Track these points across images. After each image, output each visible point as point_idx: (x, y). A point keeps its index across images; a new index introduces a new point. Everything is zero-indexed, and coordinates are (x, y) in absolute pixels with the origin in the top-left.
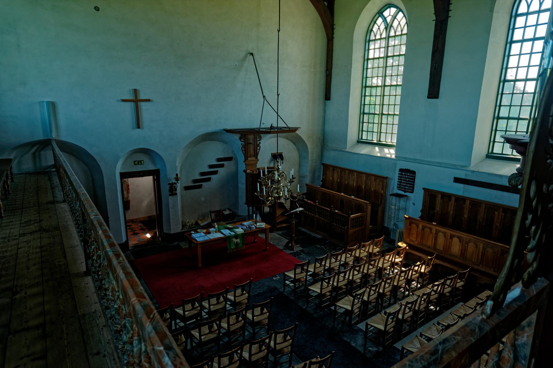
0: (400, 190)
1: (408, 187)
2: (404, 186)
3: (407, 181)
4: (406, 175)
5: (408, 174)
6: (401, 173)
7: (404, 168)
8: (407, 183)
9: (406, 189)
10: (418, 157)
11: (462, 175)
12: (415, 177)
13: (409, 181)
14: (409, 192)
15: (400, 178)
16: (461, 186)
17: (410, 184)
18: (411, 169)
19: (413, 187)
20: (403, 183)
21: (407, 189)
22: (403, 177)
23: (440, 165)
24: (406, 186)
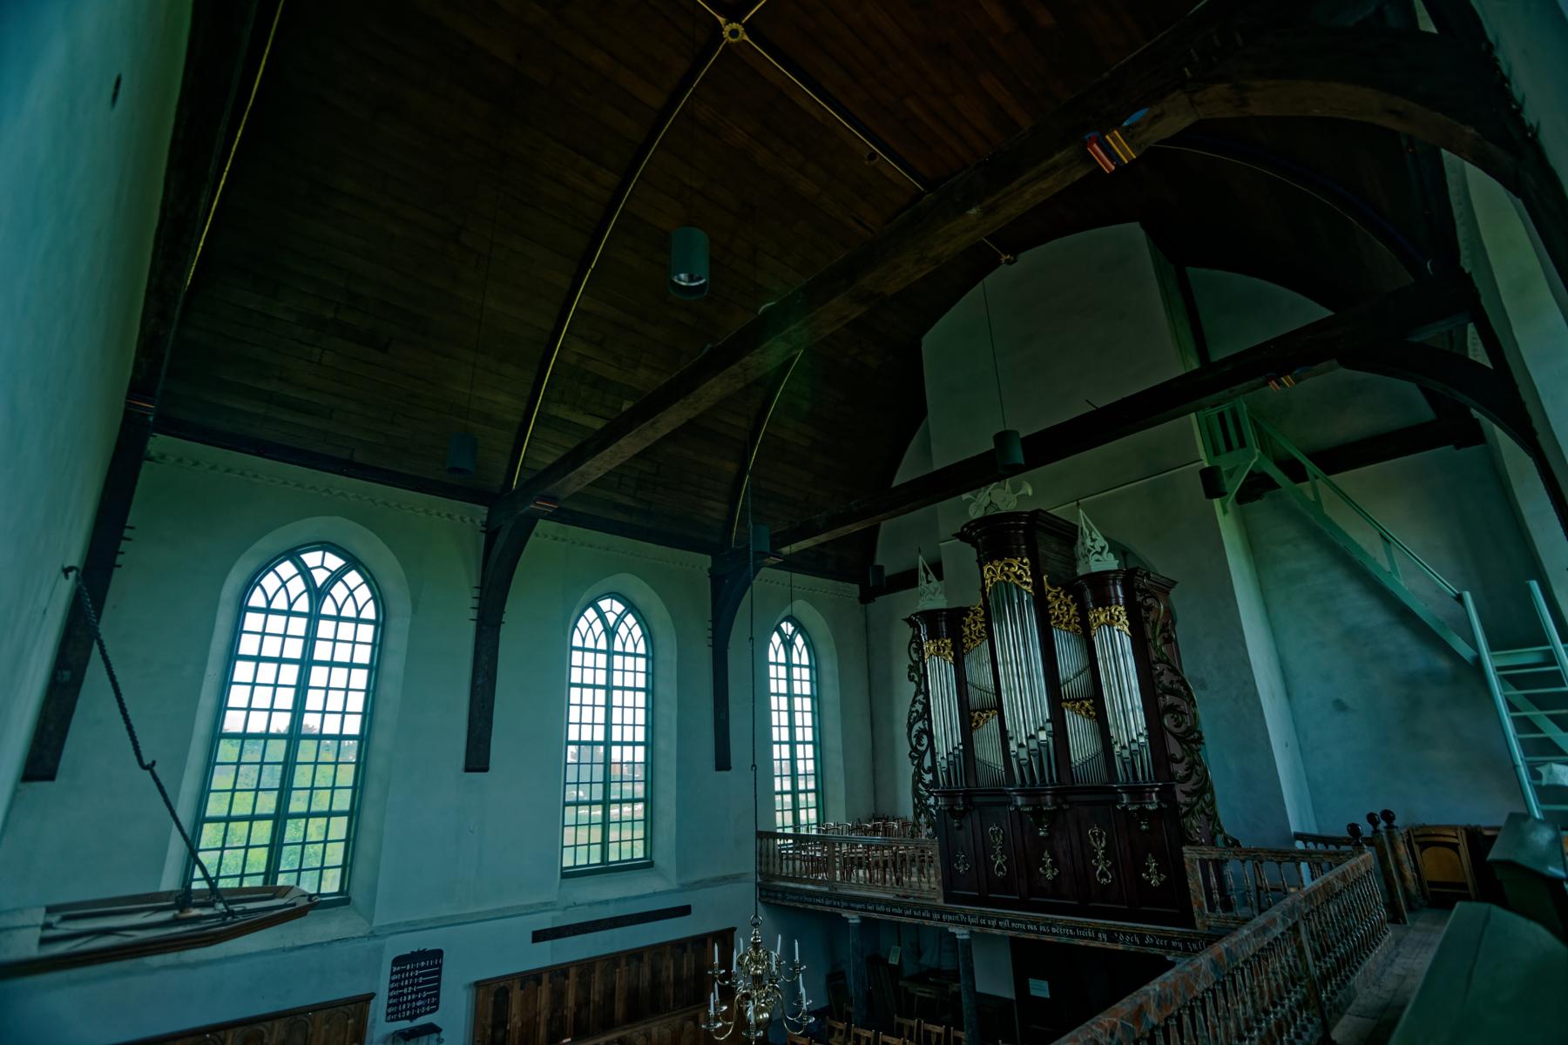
0: (397, 1019)
1: (422, 999)
2: (411, 1001)
3: (418, 984)
4: (414, 969)
5: (423, 964)
6: (398, 968)
7: (409, 953)
8: (417, 993)
9: (416, 1008)
10: (445, 911)
11: (546, 921)
12: (440, 965)
13: (424, 983)
14: (427, 1013)
15: (396, 985)
16: (547, 944)
17: (428, 990)
18: (429, 948)
19: (437, 996)
20: (407, 994)
21: (421, 1007)
22: (405, 978)
23: (501, 915)
24: (417, 1000)
